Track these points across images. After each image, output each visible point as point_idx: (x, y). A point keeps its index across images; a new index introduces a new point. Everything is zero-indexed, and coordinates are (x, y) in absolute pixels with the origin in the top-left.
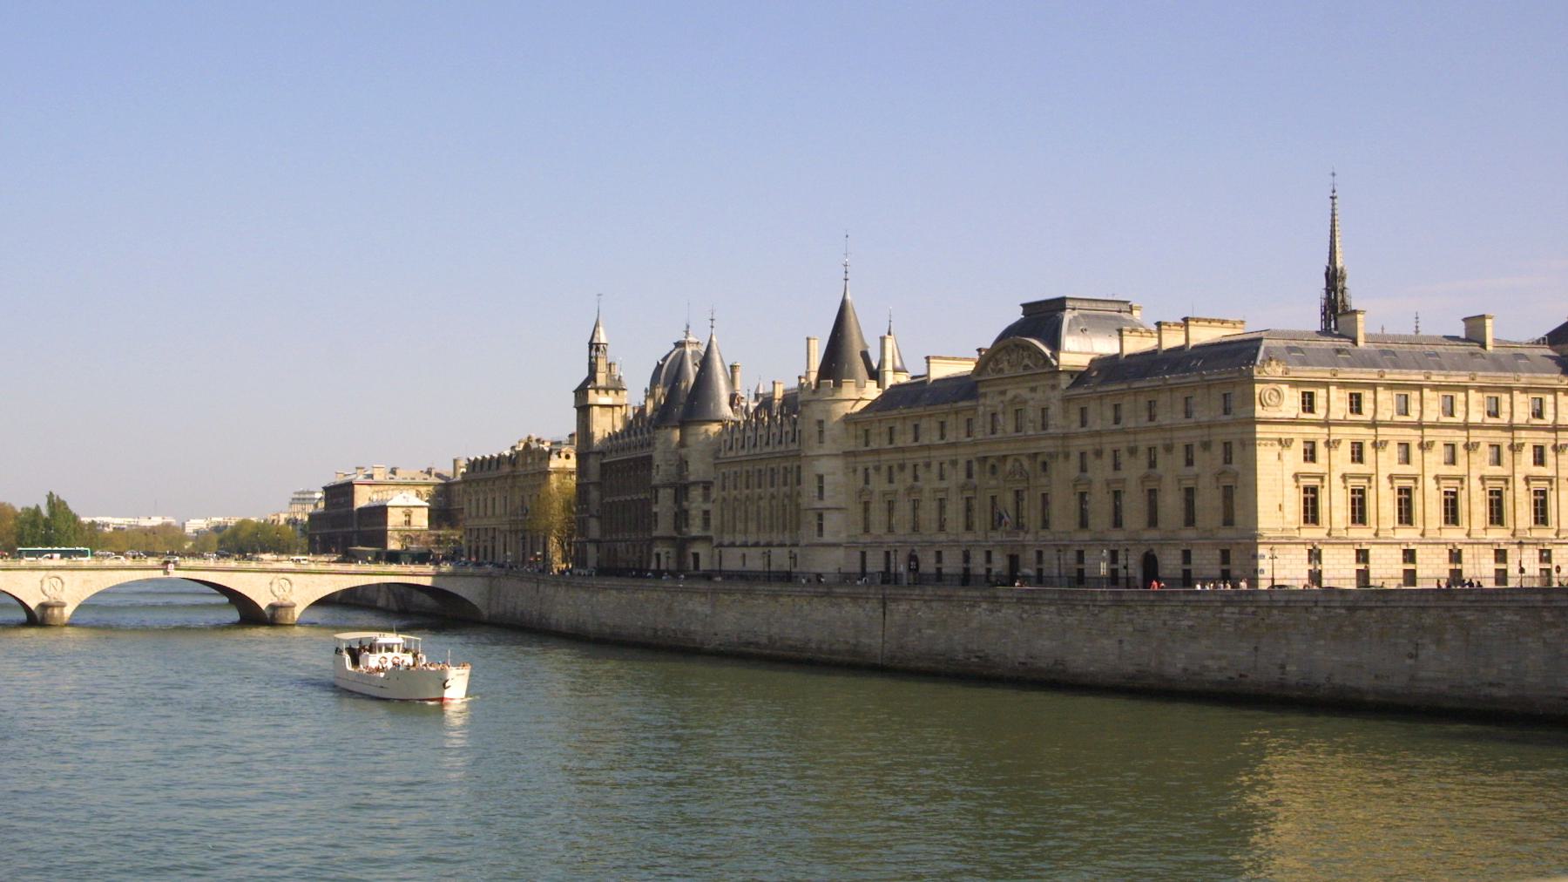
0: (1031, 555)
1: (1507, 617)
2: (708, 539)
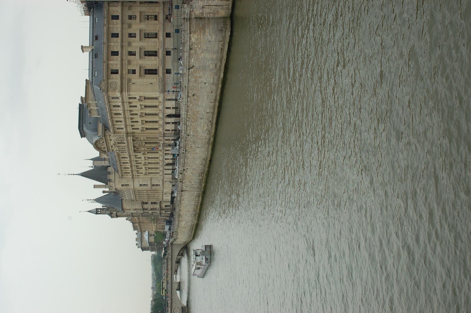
0: (167, 142)
1: (193, 61)
2: (161, 202)
